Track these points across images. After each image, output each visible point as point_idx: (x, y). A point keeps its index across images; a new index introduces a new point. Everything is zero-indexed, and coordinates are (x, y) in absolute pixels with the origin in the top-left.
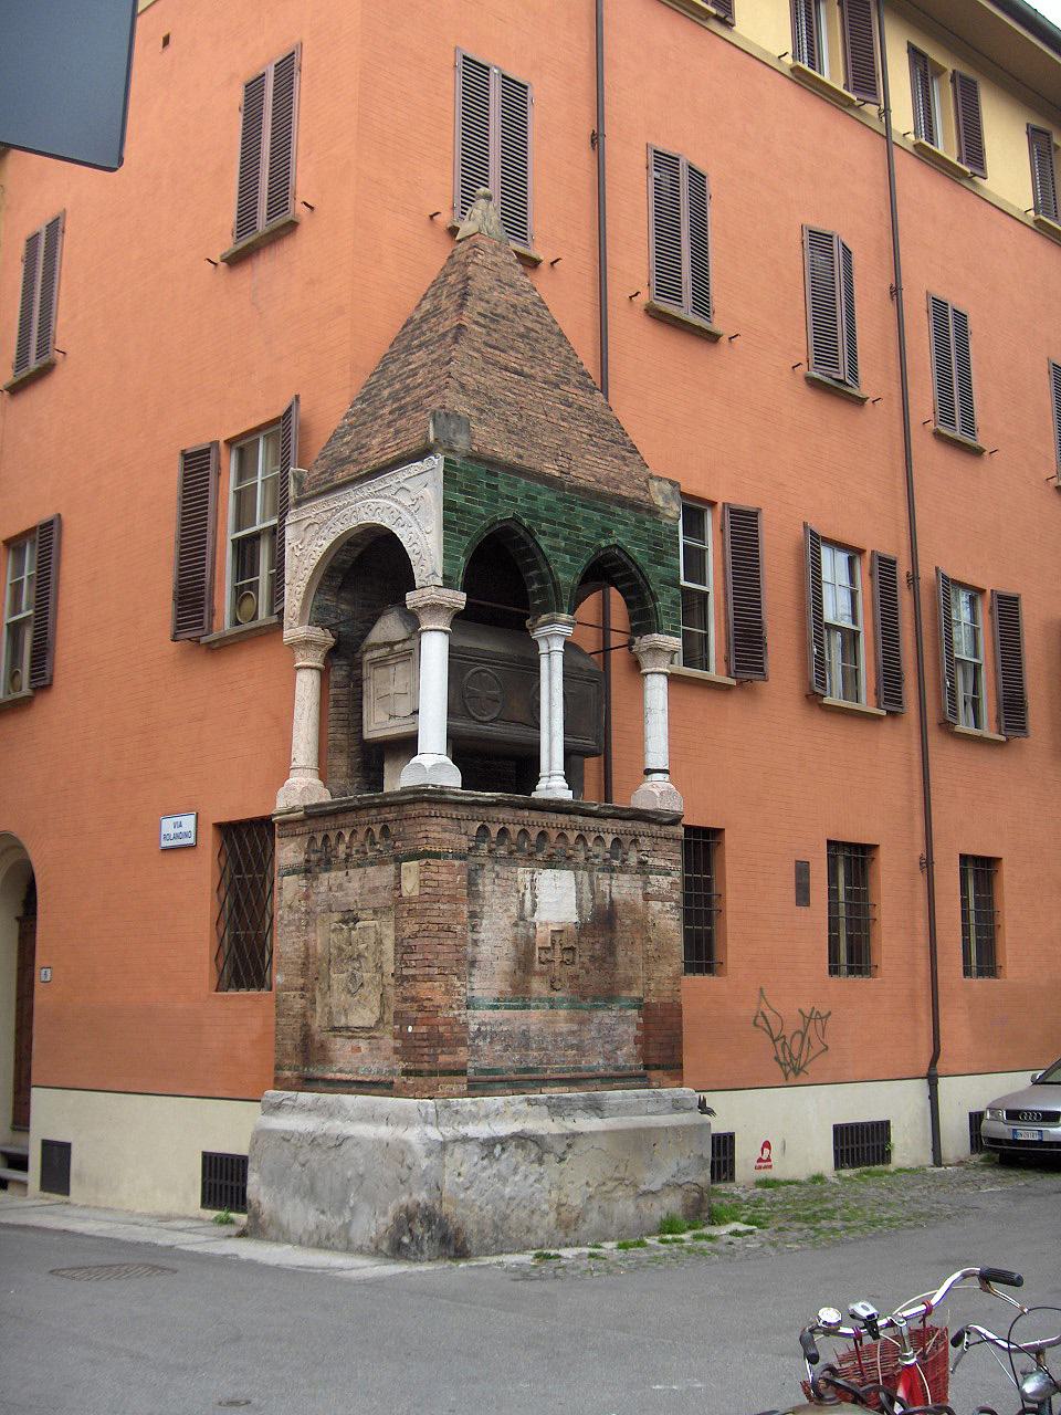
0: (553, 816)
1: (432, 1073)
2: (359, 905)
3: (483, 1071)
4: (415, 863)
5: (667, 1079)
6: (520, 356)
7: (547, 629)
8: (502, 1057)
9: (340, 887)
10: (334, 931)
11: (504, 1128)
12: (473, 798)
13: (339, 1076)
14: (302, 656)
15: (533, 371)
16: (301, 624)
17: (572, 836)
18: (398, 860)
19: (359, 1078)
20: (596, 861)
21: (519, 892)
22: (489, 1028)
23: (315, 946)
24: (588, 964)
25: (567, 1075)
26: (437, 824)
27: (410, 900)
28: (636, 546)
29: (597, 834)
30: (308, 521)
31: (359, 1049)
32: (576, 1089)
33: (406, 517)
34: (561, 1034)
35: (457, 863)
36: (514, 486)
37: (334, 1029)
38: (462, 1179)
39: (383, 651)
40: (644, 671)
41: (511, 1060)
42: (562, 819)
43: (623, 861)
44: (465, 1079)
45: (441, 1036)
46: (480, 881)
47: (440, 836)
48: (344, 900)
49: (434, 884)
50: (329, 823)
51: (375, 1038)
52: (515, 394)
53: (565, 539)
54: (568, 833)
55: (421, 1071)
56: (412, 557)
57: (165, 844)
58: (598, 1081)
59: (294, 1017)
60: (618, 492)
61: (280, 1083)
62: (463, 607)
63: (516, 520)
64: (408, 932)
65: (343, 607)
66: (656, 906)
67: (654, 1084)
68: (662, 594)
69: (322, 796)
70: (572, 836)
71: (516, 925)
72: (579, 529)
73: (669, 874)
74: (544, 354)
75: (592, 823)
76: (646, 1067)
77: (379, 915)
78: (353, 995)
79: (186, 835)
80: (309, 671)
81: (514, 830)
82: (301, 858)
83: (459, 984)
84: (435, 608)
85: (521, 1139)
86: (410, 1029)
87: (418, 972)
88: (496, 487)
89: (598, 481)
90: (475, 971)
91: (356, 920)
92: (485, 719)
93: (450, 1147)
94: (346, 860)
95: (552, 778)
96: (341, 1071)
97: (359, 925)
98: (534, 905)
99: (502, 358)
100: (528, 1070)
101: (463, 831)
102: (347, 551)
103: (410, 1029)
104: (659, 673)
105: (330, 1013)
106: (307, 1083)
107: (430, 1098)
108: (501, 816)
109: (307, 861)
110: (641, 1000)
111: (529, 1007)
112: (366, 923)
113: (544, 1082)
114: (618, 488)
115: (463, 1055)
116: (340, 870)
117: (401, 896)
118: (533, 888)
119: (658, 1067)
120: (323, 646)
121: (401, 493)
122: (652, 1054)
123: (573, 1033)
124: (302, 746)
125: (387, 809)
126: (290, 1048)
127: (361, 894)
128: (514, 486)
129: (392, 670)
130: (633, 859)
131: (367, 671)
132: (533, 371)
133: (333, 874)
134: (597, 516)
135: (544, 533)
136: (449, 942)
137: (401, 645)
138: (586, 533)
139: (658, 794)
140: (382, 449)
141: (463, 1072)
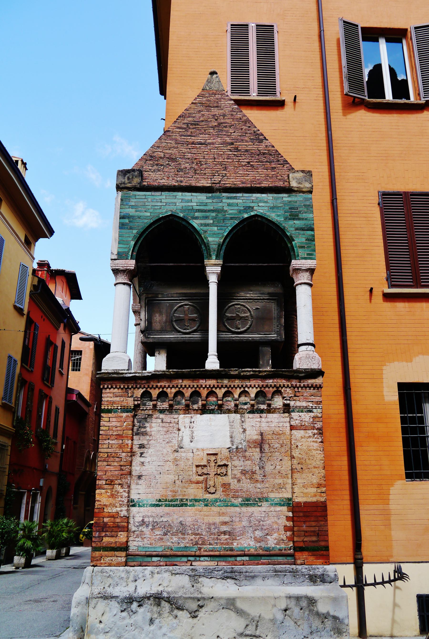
5: (311, 559)
8: (162, 539)
20: (245, 407)
21: (179, 430)
22: (151, 519)
24: (239, 475)
25: (217, 553)
29: (242, 389)
34: (214, 524)
35: (124, 415)
42: (212, 382)
45: (106, 524)
46: (147, 425)
47: (111, 399)
54: (217, 391)
66: (298, 434)
67: (299, 562)
73: (311, 411)
75: (237, 382)
76: (296, 549)
81: (171, 392)
83: (122, 490)
90: (140, 482)
93: (93, 603)
101: (130, 395)
110: (290, 499)
111: (186, 505)
115: (122, 537)
123: (225, 523)
136: (116, 464)
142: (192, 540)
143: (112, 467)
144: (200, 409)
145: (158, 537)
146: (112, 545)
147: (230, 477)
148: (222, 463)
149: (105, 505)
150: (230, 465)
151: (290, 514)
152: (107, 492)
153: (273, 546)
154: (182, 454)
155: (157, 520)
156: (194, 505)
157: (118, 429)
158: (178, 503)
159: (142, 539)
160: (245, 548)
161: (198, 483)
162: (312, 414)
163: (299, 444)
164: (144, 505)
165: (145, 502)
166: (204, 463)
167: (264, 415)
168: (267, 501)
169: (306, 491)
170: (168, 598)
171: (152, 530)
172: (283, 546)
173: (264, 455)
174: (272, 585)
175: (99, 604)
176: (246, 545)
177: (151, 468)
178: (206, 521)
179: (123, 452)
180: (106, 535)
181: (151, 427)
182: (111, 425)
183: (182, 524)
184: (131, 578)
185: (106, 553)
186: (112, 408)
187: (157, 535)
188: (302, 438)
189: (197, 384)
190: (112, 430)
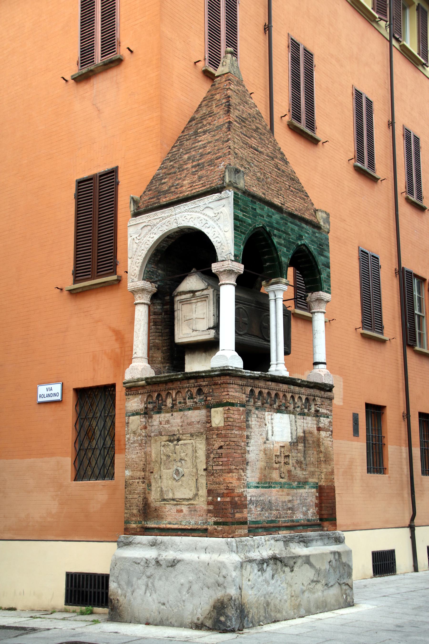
0: (281, 385)
1: (233, 524)
2: (181, 432)
3: (254, 522)
4: (221, 409)
6: (255, 141)
7: (275, 287)
9: (168, 422)
10: (164, 446)
11: (266, 553)
12: (168, 378)
13: (169, 526)
14: (139, 297)
15: (262, 150)
16: (139, 280)
17: (289, 396)
18: (209, 407)
19: (183, 527)
22: (255, 498)
23: (151, 455)
24: (295, 464)
25: (289, 524)
26: (233, 388)
27: (218, 429)
28: (313, 245)
29: (299, 395)
30: (145, 224)
31: (181, 511)
32: (292, 532)
33: (211, 222)
34: (285, 502)
35: (241, 409)
36: (262, 209)
37: (164, 500)
38: (250, 583)
39: (188, 296)
40: (313, 311)
41: (266, 516)
42: (285, 387)
43: (309, 410)
44: (246, 526)
45: (236, 503)
48: (170, 429)
49: (232, 420)
50: (162, 387)
51: (193, 504)
52: (258, 161)
53: (284, 239)
54: (287, 394)
55: (227, 522)
56: (215, 244)
57: (40, 400)
58: (301, 528)
59: (138, 494)
60: (303, 216)
61: (127, 531)
62: (242, 272)
63: (263, 228)
64: (217, 446)
65: (160, 271)
67: (325, 529)
68: (323, 271)
69: (150, 373)
70: (289, 396)
71: (265, 443)
72: (289, 235)
73: (328, 417)
74: (265, 142)
75: (297, 389)
76: (321, 519)
77: (195, 437)
78: (177, 481)
79: (55, 395)
80: (143, 305)
81: (265, 391)
82: (142, 406)
83: (243, 474)
84: (230, 272)
85: (275, 559)
86: (219, 499)
87: (224, 468)
88: (255, 209)
89: (296, 210)
91: (179, 440)
92: (241, 333)
93: (244, 565)
94: (172, 407)
95: (278, 365)
96: (170, 523)
97: (180, 442)
98: (273, 432)
99: (249, 141)
100: (272, 521)
102: (167, 241)
103: (219, 499)
104: (321, 312)
105: (162, 491)
106: (146, 531)
107: (232, 537)
108: (260, 384)
109: (146, 408)
110: (317, 483)
112: (186, 442)
113: (279, 528)
114: (304, 214)
116: (168, 412)
117: (211, 426)
118: (272, 423)
119: (327, 520)
120: (150, 292)
121: (207, 209)
122: (323, 512)
123: (290, 501)
124: (140, 346)
125: (202, 380)
126: (135, 511)
127: (182, 426)
128: (262, 209)
129: (194, 306)
130: (313, 410)
131: (177, 306)
132: (262, 150)
133: (162, 415)
134: (296, 228)
135: (275, 235)
136: (239, 452)
137: (200, 292)
138: (292, 236)
139: (323, 375)
140: (191, 187)
141: (245, 523)
142: (275, 515)
143: (237, 454)
144: (277, 409)
145: (259, 512)
146: (241, 520)
147: (291, 465)
148: (287, 454)
149: (235, 487)
150: (291, 456)
151: (317, 494)
152: (236, 476)
153: (311, 518)
154: (267, 446)
155: (258, 499)
156: (274, 487)
157: (239, 421)
158: (267, 485)
159: (251, 514)
160: (299, 520)
161: (276, 469)
162: (329, 420)
163: (324, 442)
164: (251, 486)
165: (251, 485)
166: (278, 454)
167: (305, 417)
168: (308, 485)
169: (327, 477)
170: (280, 558)
171: (256, 506)
172: (315, 518)
173: (306, 448)
174: (320, 546)
175: (248, 566)
176: (299, 518)
177: (253, 456)
178: (281, 500)
179: (243, 442)
180: (237, 511)
181: (252, 421)
182: (235, 417)
183: (270, 502)
184: (256, 546)
185: (238, 526)
186: (235, 402)
187: (258, 511)
188: (325, 437)
189: (279, 387)
190: (235, 422)
